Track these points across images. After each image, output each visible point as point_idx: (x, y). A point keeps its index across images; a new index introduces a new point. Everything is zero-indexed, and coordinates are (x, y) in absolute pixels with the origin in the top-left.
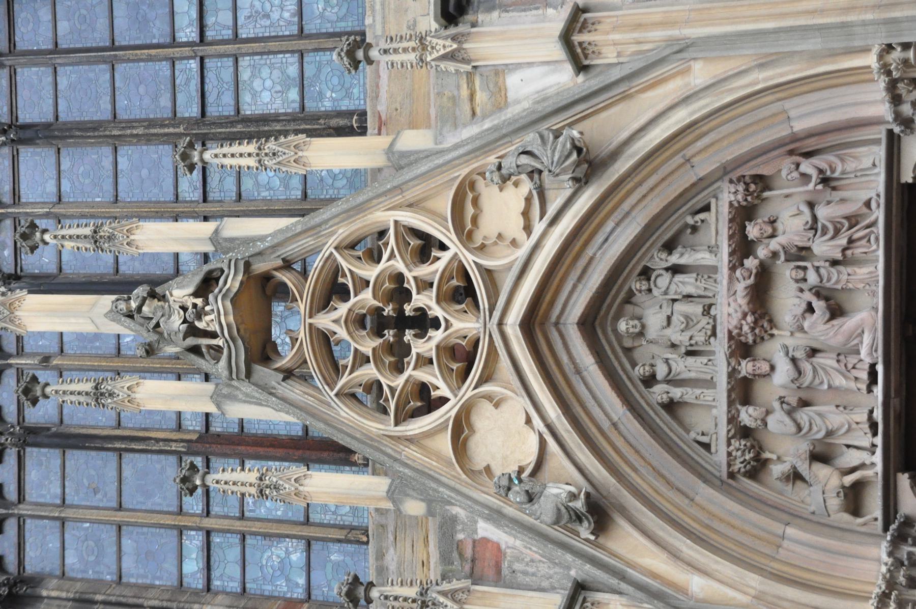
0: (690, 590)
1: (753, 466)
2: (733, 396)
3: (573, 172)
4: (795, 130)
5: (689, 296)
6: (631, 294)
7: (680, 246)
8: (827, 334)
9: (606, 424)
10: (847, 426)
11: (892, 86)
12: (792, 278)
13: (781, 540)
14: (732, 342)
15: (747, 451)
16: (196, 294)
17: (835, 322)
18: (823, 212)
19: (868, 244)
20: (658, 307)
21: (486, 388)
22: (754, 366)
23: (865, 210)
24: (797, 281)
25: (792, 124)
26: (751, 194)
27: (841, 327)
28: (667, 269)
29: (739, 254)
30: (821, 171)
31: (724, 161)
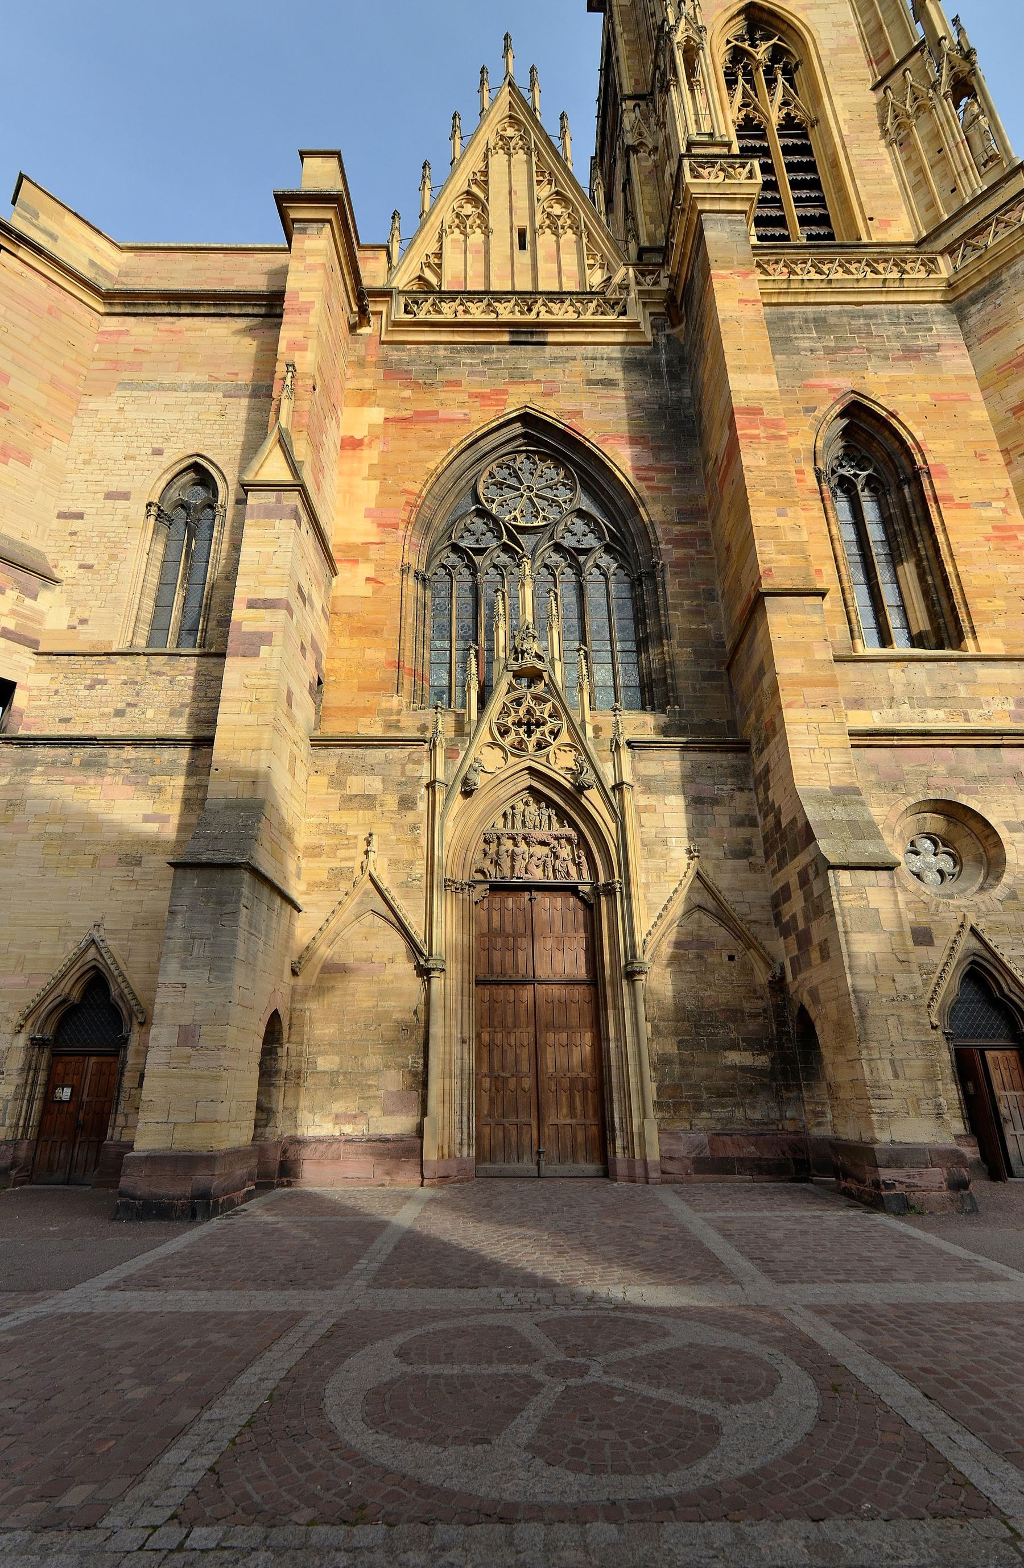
11: (608, 884)
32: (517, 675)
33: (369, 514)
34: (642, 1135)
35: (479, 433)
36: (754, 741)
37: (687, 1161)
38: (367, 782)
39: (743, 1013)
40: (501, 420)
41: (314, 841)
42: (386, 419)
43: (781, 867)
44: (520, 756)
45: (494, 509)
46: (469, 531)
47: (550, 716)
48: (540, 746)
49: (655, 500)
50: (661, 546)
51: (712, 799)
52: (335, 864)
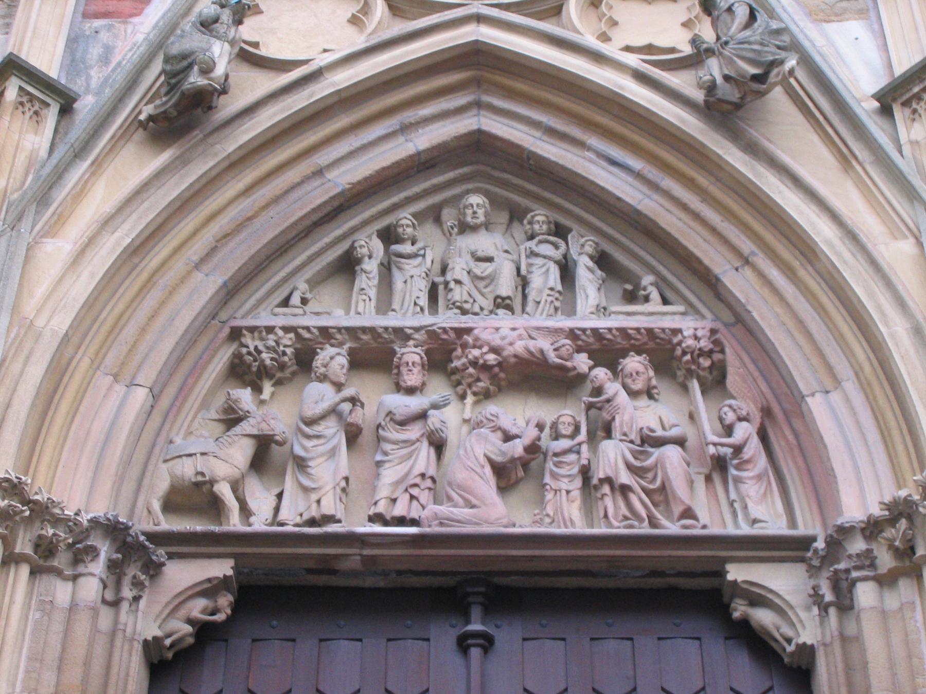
0: (49, 240)
1: (250, 366)
2: (365, 337)
3: (727, 78)
4: (809, 400)
7: (604, 274)
8: (468, 459)
10: (313, 486)
12: (558, 418)
13: (127, 383)
14: (452, 335)
15: (276, 356)
17: (488, 470)
18: (672, 453)
19: (621, 518)
20: (506, 248)
22: (413, 363)
23: (677, 510)
24: (554, 426)
25: (817, 395)
26: (694, 361)
27: (481, 477)
28: (565, 256)
29: (596, 346)
31: (749, 308)
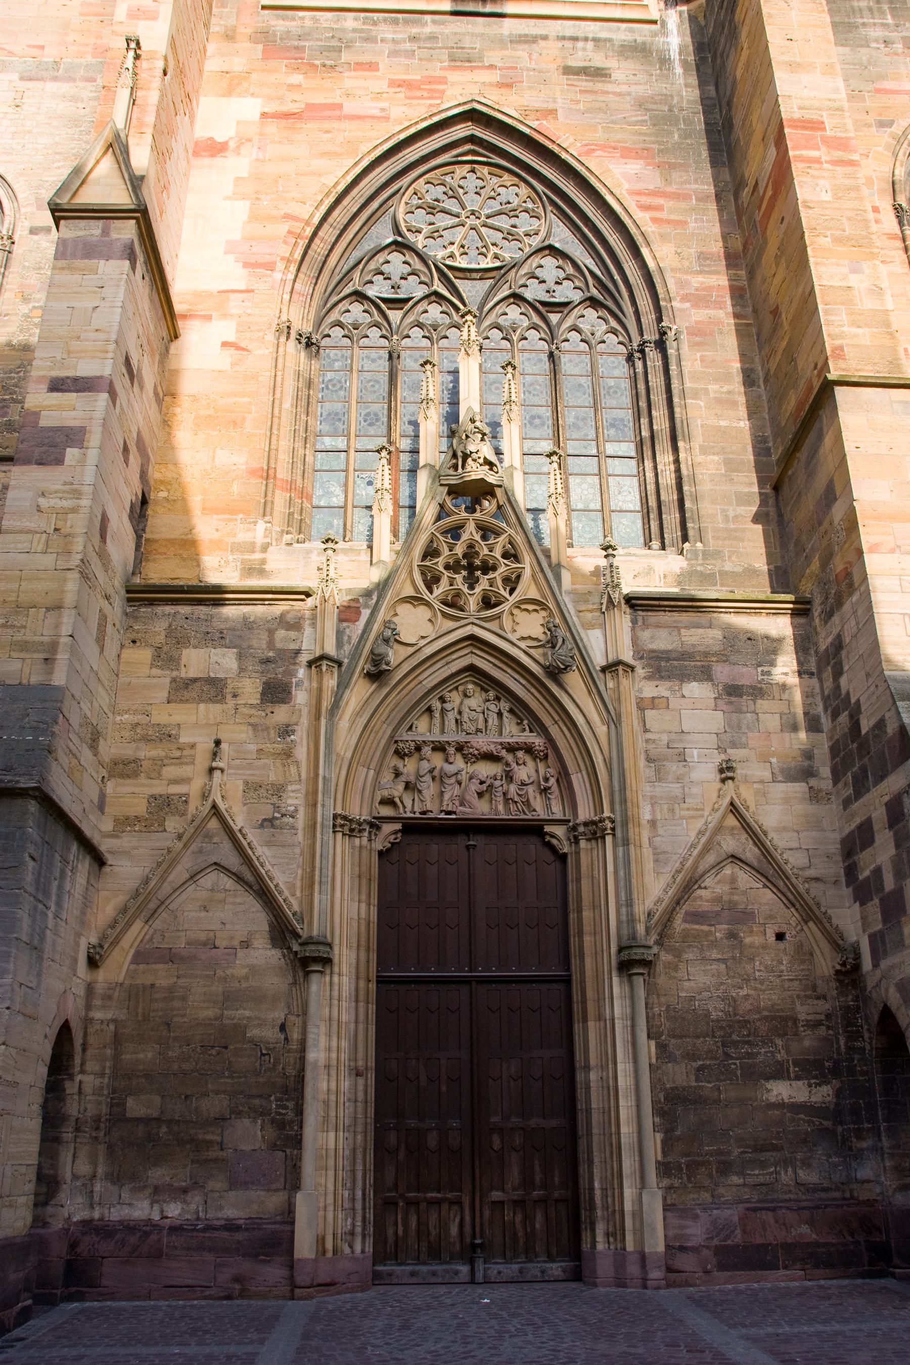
5: (486, 721)
6: (486, 691)
9: (421, 678)
11: (593, 823)
16: (485, 458)
21: (439, 613)
30: (549, 788)
32: (454, 491)
33: (231, 248)
34: (638, 1214)
35: (402, 136)
36: (817, 601)
37: (706, 1253)
38: (214, 659)
39: (795, 1020)
40: (436, 119)
41: (128, 751)
42: (264, 115)
43: (858, 794)
44: (457, 619)
45: (419, 241)
46: (382, 273)
47: (505, 555)
48: (487, 602)
49: (663, 237)
50: (674, 304)
51: (753, 688)
52: (159, 788)
